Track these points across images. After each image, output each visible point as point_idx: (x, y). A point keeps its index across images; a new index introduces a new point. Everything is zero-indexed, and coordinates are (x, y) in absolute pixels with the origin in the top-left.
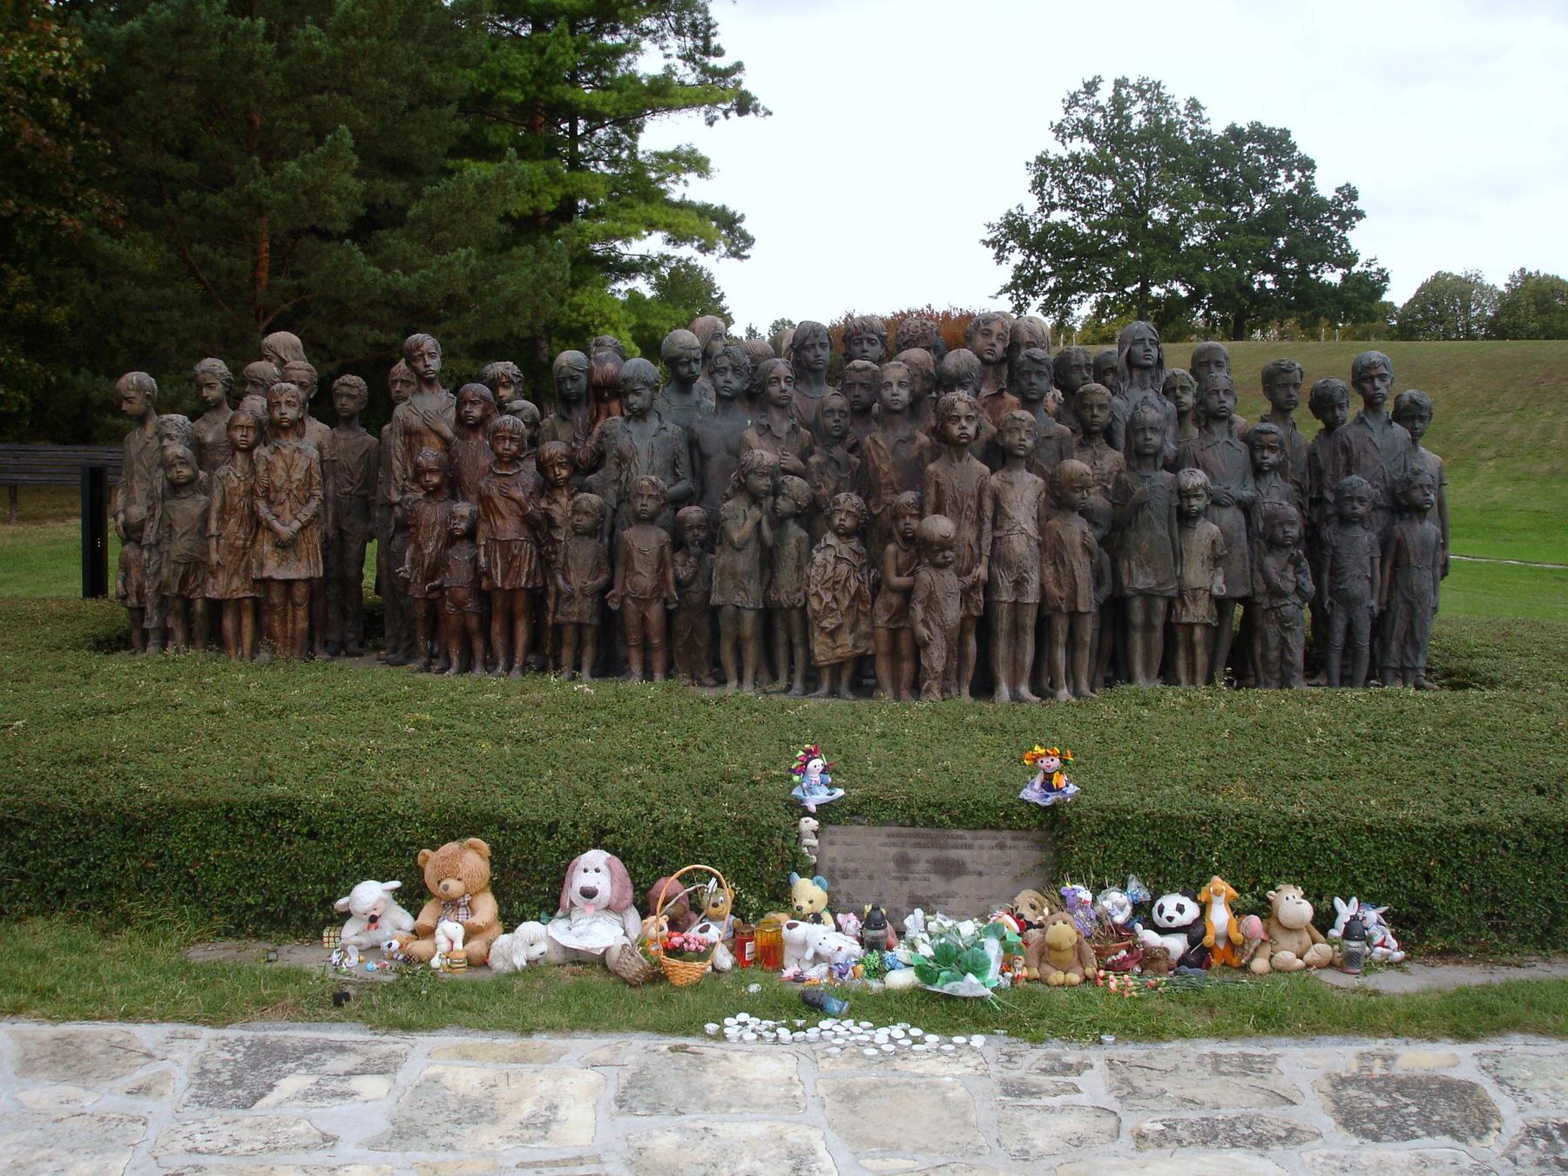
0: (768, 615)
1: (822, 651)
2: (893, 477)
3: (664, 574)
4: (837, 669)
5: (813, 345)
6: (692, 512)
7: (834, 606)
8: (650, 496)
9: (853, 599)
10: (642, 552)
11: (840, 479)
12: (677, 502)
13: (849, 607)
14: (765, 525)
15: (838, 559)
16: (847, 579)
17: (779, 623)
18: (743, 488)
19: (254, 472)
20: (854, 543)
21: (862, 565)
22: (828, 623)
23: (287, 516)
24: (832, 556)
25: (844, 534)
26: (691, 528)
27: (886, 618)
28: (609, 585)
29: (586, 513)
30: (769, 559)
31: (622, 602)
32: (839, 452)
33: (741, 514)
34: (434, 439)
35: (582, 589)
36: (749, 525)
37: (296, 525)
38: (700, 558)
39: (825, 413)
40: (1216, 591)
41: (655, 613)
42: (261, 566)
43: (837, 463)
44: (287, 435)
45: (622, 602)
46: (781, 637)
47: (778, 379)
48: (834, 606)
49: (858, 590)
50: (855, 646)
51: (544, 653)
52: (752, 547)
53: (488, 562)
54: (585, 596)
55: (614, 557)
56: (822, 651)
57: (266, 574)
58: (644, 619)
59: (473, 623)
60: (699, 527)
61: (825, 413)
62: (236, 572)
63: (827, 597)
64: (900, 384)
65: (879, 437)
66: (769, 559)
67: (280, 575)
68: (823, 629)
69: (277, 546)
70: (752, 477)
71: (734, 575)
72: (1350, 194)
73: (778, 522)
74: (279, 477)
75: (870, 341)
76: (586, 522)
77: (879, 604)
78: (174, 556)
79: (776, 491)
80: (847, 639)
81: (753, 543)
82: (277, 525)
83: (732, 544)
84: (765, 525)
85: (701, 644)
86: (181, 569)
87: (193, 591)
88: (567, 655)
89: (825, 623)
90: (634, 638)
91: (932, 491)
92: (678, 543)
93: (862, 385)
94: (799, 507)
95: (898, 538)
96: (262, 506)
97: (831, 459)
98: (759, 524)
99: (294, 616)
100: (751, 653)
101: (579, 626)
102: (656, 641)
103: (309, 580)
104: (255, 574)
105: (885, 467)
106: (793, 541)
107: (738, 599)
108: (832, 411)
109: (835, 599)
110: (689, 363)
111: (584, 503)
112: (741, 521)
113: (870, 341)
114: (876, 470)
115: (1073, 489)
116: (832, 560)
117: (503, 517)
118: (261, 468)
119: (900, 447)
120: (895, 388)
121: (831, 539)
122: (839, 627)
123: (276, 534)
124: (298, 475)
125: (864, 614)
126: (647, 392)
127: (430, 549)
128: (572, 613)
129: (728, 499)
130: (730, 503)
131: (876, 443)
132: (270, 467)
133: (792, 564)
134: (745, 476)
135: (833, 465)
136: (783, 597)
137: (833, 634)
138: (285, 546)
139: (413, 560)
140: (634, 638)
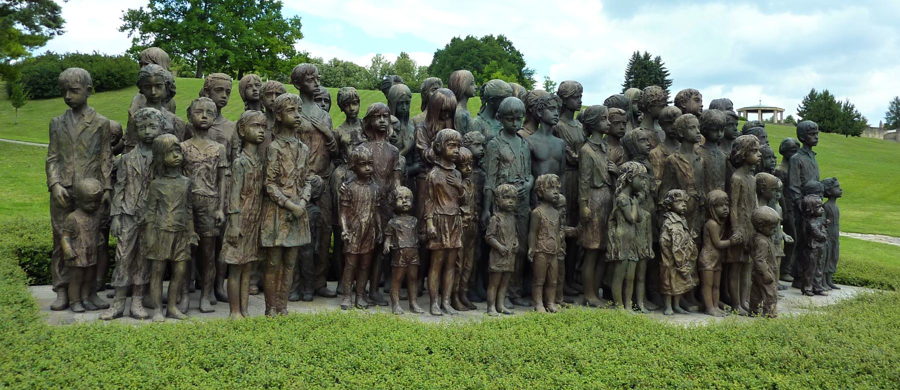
4: (686, 295)
10: (551, 224)
15: (684, 229)
19: (265, 162)
23: (296, 197)
27: (713, 265)
34: (318, 136)
37: (303, 202)
40: (787, 240)
41: (555, 263)
42: (274, 236)
44: (291, 134)
45: (534, 257)
51: (473, 291)
53: (438, 229)
54: (514, 253)
55: (527, 227)
57: (278, 243)
58: (549, 267)
59: (413, 272)
61: (639, 140)
62: (247, 241)
67: (286, 245)
68: (680, 273)
69: (288, 220)
72: (297, 22)
74: (289, 167)
78: (164, 226)
82: (290, 204)
83: (629, 222)
86: (172, 238)
87: (178, 254)
88: (492, 292)
91: (738, 191)
95: (716, 217)
96: (274, 190)
99: (284, 275)
101: (504, 273)
103: (301, 249)
104: (266, 243)
114: (685, 175)
115: (772, 190)
117: (450, 199)
118: (273, 159)
119: (696, 163)
123: (289, 210)
124: (301, 165)
127: (365, 217)
131: (681, 159)
132: (280, 157)
133: (644, 232)
134: (632, 178)
138: (293, 219)
139: (349, 226)
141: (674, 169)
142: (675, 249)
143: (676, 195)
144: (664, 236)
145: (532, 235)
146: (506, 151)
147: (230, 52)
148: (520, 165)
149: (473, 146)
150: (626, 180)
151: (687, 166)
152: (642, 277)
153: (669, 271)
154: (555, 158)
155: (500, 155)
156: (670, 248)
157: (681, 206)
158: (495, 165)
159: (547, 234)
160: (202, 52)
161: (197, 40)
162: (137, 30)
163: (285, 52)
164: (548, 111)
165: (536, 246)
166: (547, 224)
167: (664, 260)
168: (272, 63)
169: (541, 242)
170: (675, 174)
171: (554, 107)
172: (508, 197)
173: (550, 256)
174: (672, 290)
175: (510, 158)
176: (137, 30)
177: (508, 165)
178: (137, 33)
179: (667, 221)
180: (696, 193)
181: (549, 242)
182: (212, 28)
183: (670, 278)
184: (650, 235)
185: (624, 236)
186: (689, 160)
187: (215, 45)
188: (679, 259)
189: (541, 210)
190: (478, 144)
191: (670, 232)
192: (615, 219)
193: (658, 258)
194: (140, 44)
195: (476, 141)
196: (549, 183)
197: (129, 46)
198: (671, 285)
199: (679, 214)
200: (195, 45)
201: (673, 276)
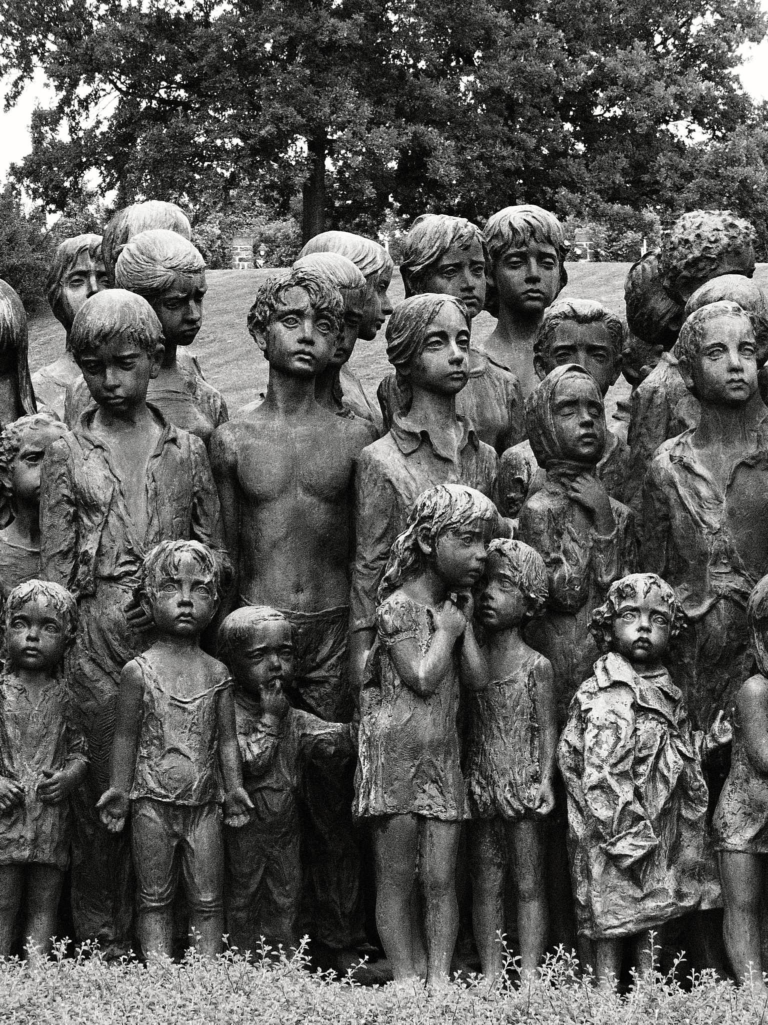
0: (469, 834)
1: (613, 909)
2: (729, 538)
3: (218, 753)
5: (459, 267)
6: (257, 617)
7: (637, 808)
8: (195, 585)
9: (671, 798)
10: (178, 705)
11: (598, 545)
12: (232, 590)
13: (665, 812)
14: (471, 647)
15: (639, 709)
16: (661, 751)
17: (488, 850)
18: (421, 563)
20: (663, 681)
21: (682, 723)
22: (628, 847)
24: (614, 703)
25: (644, 660)
26: (265, 651)
27: (750, 833)
28: (94, 777)
29: (44, 622)
30: (472, 711)
31: (130, 816)
32: (588, 489)
33: (424, 619)
35: (43, 788)
36: (440, 643)
38: (281, 715)
39: (557, 409)
41: (202, 837)
43: (589, 513)
46: (493, 879)
47: (444, 336)
48: (637, 808)
49: (682, 777)
50: (680, 895)
52: (448, 689)
54: (48, 803)
56: (613, 909)
58: (181, 850)
60: (279, 650)
61: (557, 409)
63: (625, 792)
64: (742, 347)
65: (693, 456)
66: (472, 711)
68: (613, 860)
70: (447, 542)
71: (416, 751)
73: (489, 633)
75: (541, 257)
76: (47, 640)
77: (731, 804)
79: (489, 571)
80: (665, 879)
81: (447, 683)
83: (411, 685)
84: (471, 647)
85: (283, 901)
89: (622, 847)
90: (155, 892)
92: (244, 688)
93: (591, 350)
94: (530, 603)
97: (574, 502)
98: (457, 647)
100: (443, 919)
102: (207, 897)
105: (714, 519)
106: (522, 677)
107: (422, 800)
108: (573, 403)
109: (638, 795)
110: (184, 302)
111: (42, 600)
112: (426, 635)
113: (541, 257)
114: (695, 524)
116: (629, 714)
120: (734, 358)
121: (616, 666)
122: (649, 857)
125: (693, 825)
126: (142, 363)
128: (18, 843)
129: (392, 588)
130: (399, 598)
131: (688, 468)
133: (519, 725)
135: (578, 516)
136: (504, 794)
137: (635, 873)
140: (155, 892)
141: (666, 501)
142: (592, 776)
143: (621, 595)
144: (570, 734)
145: (121, 745)
146: (93, 475)
147: (432, 134)
148: (142, 518)
149: (21, 465)
150: (415, 549)
151: (704, 491)
152: (528, 883)
153: (585, 852)
154: (309, 489)
155: (74, 487)
156: (579, 772)
157: (630, 632)
158: (62, 523)
159: (161, 738)
160: (320, 146)
161: (287, 98)
162: (39, 72)
163: (699, 112)
164: (279, 326)
165: (133, 777)
166: (163, 707)
167: (574, 818)
168: (639, 167)
169: (144, 768)
170: (668, 517)
171: (300, 313)
172: (27, 621)
173: (179, 813)
174: (592, 918)
175: (103, 495)
176: (39, 72)
177: (98, 519)
178: (42, 92)
179: (588, 685)
180: (738, 583)
181: (166, 764)
182: (345, 30)
183: (588, 874)
184: (548, 734)
185: (390, 737)
186: (712, 463)
187: (367, 110)
188: (602, 812)
189: (150, 665)
190: (35, 457)
191: (583, 720)
192: (376, 682)
193: (560, 811)
194: (63, 135)
195: (28, 447)
196: (164, 568)
197: (21, 148)
198: (589, 906)
199: (628, 654)
200: (277, 119)
201: (597, 870)
